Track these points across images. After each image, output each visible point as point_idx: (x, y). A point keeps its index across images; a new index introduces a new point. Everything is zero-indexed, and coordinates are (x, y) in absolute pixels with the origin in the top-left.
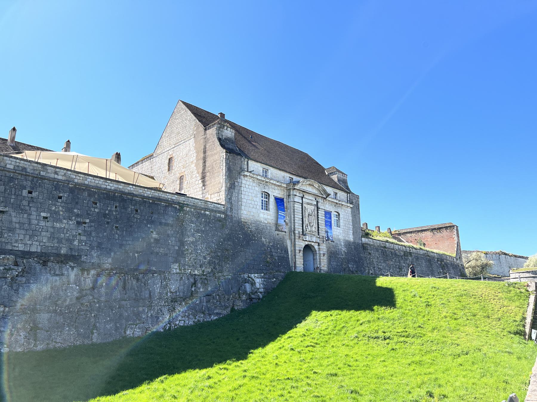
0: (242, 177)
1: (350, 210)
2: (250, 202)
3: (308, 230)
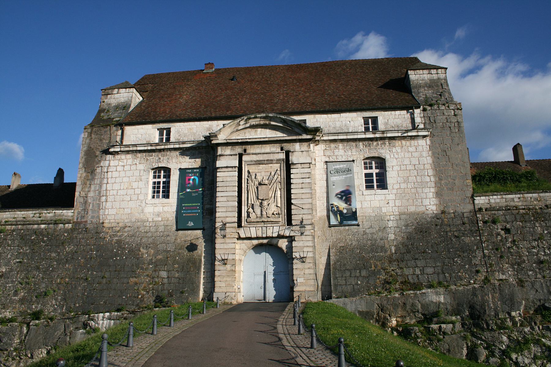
1: (424, 144)
3: (253, 216)
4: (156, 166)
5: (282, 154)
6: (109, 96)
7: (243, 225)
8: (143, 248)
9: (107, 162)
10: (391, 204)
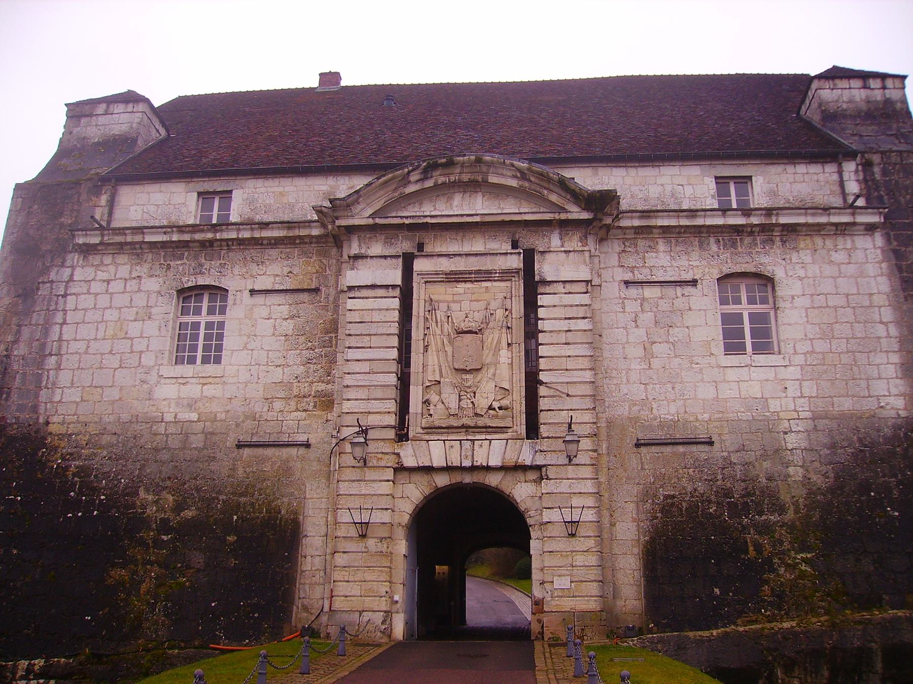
0: (74, 258)
2: (106, 346)
4: (190, 284)
5: (515, 257)
6: (83, 120)
7: (411, 435)
8: (147, 490)
9: (67, 272)
10: (793, 391)
